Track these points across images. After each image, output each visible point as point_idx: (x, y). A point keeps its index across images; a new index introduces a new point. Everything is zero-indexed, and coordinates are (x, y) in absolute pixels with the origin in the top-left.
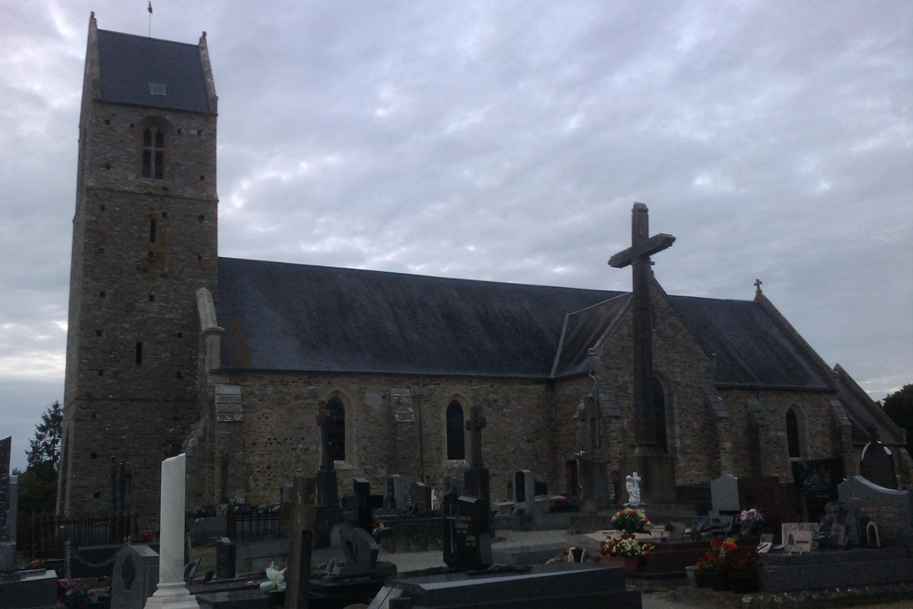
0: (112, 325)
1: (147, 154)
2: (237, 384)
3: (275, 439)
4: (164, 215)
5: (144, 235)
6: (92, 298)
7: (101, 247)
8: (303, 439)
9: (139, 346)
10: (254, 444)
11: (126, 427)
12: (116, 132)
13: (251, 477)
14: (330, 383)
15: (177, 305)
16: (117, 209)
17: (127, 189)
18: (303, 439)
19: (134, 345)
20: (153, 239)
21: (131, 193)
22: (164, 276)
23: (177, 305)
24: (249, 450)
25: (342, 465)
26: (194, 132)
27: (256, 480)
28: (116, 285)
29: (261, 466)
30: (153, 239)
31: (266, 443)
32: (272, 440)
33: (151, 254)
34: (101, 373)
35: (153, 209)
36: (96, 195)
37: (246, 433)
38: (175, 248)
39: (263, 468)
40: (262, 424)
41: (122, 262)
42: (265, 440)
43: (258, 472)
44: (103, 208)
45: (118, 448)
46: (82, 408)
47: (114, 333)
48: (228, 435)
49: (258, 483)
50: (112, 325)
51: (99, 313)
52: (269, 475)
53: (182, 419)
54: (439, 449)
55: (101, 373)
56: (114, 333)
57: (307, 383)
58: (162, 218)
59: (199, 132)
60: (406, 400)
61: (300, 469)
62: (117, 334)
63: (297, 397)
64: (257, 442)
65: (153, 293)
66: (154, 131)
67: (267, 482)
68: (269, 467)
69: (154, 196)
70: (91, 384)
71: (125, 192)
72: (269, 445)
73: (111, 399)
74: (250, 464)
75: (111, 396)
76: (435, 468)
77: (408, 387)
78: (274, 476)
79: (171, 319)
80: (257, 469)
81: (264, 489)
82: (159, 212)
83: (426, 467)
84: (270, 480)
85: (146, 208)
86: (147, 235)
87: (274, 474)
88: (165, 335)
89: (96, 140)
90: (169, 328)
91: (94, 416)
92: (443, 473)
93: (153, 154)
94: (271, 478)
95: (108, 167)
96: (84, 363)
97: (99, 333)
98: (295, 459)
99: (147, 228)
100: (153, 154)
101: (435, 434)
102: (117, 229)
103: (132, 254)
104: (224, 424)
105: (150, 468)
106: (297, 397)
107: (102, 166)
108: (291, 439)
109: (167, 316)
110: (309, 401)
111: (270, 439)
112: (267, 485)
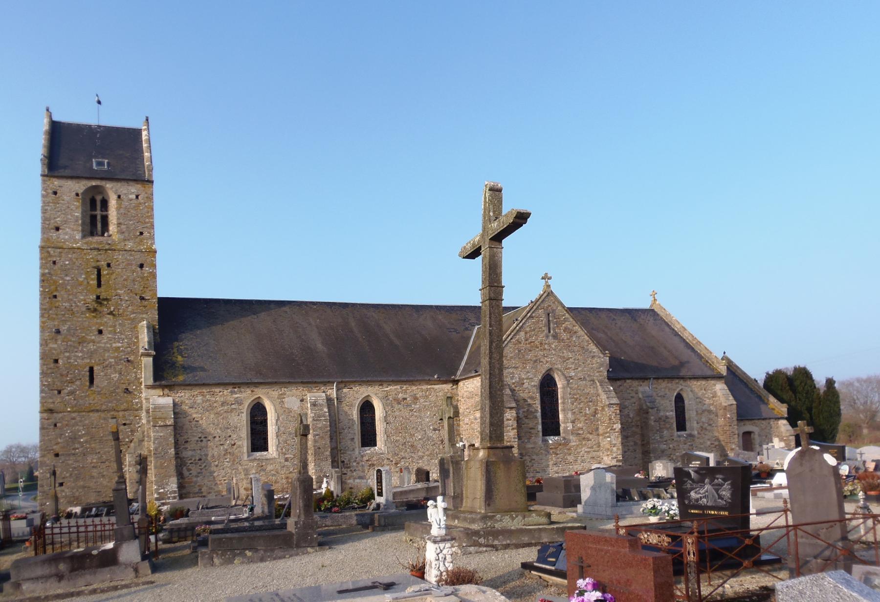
0: (67, 354)
1: (93, 218)
2: (168, 396)
3: (206, 437)
4: (109, 265)
5: (91, 282)
6: (48, 334)
7: (55, 294)
8: (230, 436)
9: (91, 370)
10: (186, 442)
11: (83, 432)
12: (63, 200)
13: (185, 468)
14: (252, 391)
15: (123, 336)
16: (67, 263)
17: (74, 245)
18: (230, 436)
19: (87, 369)
20: (99, 285)
21: (78, 248)
22: (111, 313)
23: (123, 336)
24: (183, 447)
25: (266, 455)
26: (134, 197)
27: (189, 470)
28: (69, 323)
29: (193, 459)
30: (99, 285)
31: (197, 441)
32: (202, 439)
33: (98, 297)
34: (59, 392)
35: (98, 261)
36: (48, 252)
37: (179, 434)
38: (119, 291)
39: (195, 460)
40: (193, 426)
41: (73, 305)
42: (197, 439)
43: (191, 463)
44: (54, 263)
45: (76, 449)
46: (45, 419)
47: (69, 361)
48: (161, 436)
49: (191, 472)
50: (67, 354)
51: (55, 346)
52: (200, 466)
53: (131, 424)
54: (353, 439)
55: (59, 392)
56: (69, 361)
57: (232, 393)
58: (106, 268)
59: (137, 197)
60: (320, 402)
61: (228, 460)
62: (72, 361)
63: (223, 404)
64: (189, 440)
65: (102, 328)
66: (99, 198)
67: (199, 471)
68: (200, 460)
69: (99, 250)
70: (51, 401)
71: (74, 248)
72: (200, 442)
73: (69, 412)
74: (184, 458)
75: (69, 409)
76: (350, 454)
77: (324, 392)
78: (205, 466)
79: (119, 348)
80: (190, 462)
81: (197, 476)
82: (103, 263)
83: (341, 454)
84: (201, 469)
85: (92, 260)
86: (95, 282)
87: (205, 464)
88: (113, 360)
89: (46, 208)
90: (116, 354)
91: (55, 425)
92: (356, 458)
93: (99, 218)
94: (202, 467)
95: (57, 229)
96: (44, 385)
97: (56, 361)
98: (223, 452)
99: (94, 276)
100: (99, 218)
101: (349, 428)
102: (68, 278)
103: (82, 298)
104: (157, 428)
105: (104, 462)
106: (223, 404)
107: (52, 229)
108: (219, 437)
109: (114, 345)
110: (233, 406)
111: (200, 438)
112: (199, 473)
